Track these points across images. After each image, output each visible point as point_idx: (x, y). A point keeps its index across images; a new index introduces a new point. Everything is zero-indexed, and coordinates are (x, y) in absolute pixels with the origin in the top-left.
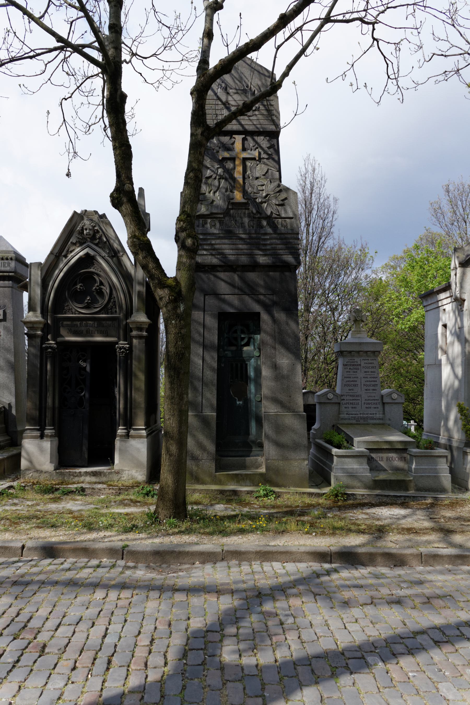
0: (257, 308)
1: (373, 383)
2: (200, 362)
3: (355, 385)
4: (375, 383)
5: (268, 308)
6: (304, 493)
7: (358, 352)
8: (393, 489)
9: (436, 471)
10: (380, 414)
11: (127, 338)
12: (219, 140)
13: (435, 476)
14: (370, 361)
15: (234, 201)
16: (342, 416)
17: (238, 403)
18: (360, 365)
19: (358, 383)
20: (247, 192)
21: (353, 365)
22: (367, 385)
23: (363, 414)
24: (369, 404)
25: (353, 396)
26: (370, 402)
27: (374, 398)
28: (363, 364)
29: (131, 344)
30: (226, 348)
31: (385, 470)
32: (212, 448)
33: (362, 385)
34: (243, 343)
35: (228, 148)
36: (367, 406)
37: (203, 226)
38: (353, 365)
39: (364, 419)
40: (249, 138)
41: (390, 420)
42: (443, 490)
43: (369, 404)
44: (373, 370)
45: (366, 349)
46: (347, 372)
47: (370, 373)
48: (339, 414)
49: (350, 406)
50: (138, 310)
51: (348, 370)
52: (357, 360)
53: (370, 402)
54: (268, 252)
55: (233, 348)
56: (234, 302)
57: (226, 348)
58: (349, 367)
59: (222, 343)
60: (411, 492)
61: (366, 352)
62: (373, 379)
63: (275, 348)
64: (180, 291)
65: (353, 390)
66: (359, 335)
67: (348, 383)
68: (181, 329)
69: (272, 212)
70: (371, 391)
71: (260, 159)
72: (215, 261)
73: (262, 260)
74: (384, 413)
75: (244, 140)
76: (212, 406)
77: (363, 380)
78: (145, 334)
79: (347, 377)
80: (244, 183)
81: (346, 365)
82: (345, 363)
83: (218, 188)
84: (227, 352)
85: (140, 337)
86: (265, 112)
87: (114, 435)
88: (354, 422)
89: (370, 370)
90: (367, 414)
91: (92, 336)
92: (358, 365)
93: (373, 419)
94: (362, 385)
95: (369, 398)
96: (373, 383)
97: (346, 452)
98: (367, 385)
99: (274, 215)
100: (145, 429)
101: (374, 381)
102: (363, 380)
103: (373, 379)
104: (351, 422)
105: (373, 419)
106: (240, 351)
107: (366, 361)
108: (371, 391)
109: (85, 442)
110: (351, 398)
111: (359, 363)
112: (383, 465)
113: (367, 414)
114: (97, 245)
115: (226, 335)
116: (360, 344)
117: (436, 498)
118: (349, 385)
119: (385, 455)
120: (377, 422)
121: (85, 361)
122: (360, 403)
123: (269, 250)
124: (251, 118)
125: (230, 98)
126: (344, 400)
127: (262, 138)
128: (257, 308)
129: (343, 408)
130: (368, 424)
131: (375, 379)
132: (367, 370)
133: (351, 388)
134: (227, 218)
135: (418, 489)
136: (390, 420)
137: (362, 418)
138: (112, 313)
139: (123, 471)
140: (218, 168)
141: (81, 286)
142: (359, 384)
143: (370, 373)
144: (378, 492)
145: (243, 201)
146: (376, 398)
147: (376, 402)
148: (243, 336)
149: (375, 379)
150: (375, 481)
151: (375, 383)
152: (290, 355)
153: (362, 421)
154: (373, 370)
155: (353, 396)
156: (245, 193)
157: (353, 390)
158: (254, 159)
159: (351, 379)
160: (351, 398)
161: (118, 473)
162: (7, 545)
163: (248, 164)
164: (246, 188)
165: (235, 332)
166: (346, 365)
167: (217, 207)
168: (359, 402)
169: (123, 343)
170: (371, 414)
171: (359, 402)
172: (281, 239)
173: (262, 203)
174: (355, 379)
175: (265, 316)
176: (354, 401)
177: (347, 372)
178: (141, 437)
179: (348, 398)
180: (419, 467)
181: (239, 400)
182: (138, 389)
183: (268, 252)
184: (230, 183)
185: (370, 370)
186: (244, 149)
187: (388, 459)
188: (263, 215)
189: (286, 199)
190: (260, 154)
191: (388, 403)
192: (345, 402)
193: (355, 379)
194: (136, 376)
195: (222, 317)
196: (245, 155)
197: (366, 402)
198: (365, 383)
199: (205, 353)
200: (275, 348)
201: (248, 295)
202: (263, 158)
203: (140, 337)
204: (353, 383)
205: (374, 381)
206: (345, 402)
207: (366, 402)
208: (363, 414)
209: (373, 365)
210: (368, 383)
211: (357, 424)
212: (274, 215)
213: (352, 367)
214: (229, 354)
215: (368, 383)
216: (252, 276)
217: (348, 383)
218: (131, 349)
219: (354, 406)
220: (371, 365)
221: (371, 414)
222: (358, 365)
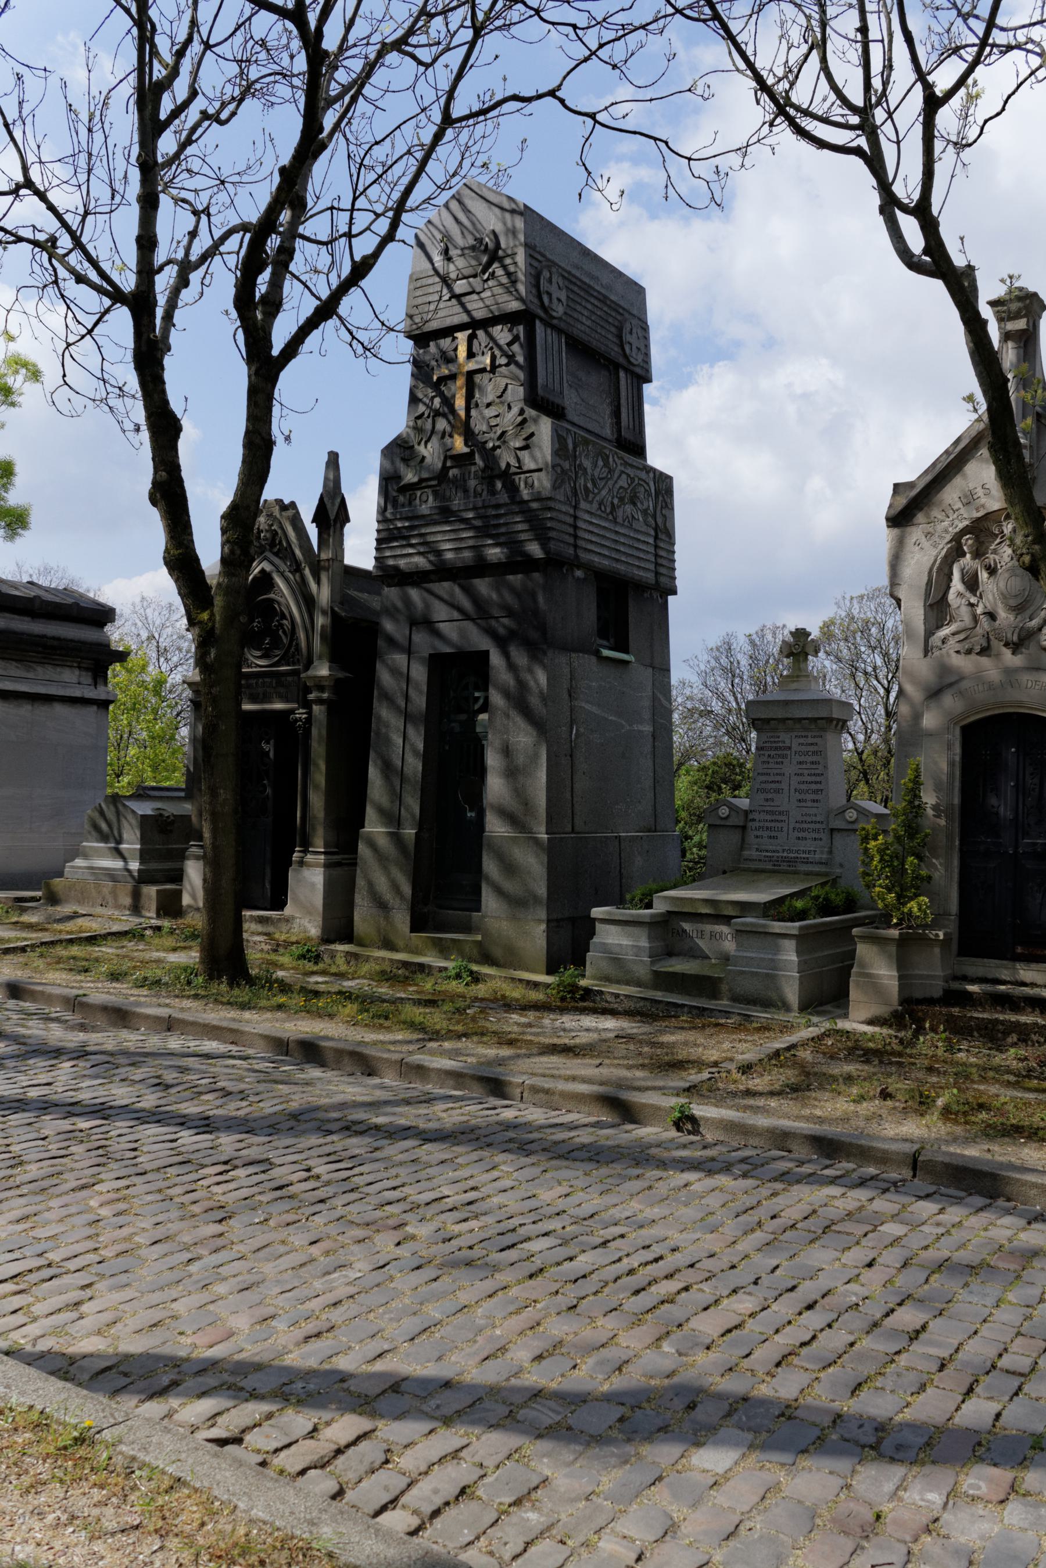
0: (484, 643)
1: (814, 787)
2: (400, 741)
3: (777, 791)
4: (818, 786)
5: (502, 643)
6: (521, 980)
7: (784, 720)
8: (688, 993)
9: (774, 965)
10: (822, 853)
11: (307, 705)
12: (438, 346)
13: (767, 975)
14: (810, 740)
15: (454, 452)
16: (746, 853)
18: (790, 748)
19: (784, 786)
20: (473, 433)
21: (776, 748)
22: (801, 791)
23: (790, 851)
24: (803, 830)
25: (772, 813)
26: (805, 826)
27: (814, 819)
28: (795, 747)
29: (310, 713)
31: (707, 957)
32: (407, 889)
34: (476, 707)
35: (449, 358)
36: (800, 835)
37: (410, 504)
38: (776, 748)
39: (790, 861)
40: (481, 333)
41: (841, 865)
42: (786, 1007)
43: (803, 830)
44: (814, 759)
45: (798, 713)
47: (809, 766)
48: (742, 848)
49: (766, 834)
50: (320, 658)
51: (765, 759)
52: (785, 737)
53: (805, 826)
54: (502, 539)
55: (463, 717)
56: (456, 632)
60: (724, 1003)
61: (800, 720)
62: (813, 779)
63: (508, 716)
64: (213, 628)
65: (772, 800)
66: (794, 686)
67: (763, 786)
68: (211, 687)
69: (508, 465)
70: (809, 804)
71: (494, 367)
72: (420, 562)
73: (494, 553)
74: (830, 852)
75: (471, 339)
77: (795, 780)
78: (325, 695)
80: (468, 415)
83: (433, 431)
85: (320, 701)
86: (504, 280)
87: (290, 863)
88: (770, 867)
89: (810, 759)
90: (797, 852)
91: (271, 702)
93: (807, 862)
95: (805, 818)
96: (814, 787)
97: (609, 913)
98: (801, 791)
99: (513, 470)
100: (324, 853)
101: (816, 783)
102: (795, 780)
103: (813, 779)
104: (761, 866)
105: (807, 862)
106: (472, 722)
107: (802, 740)
108: (809, 804)
109: (268, 871)
110: (769, 817)
112: (703, 947)
113: (797, 852)
114: (276, 554)
116: (787, 703)
117: (749, 1016)
118: (764, 791)
119: (708, 928)
120: (817, 868)
121: (268, 742)
122: (785, 829)
123: (503, 534)
124: (483, 295)
125: (452, 267)
126: (754, 820)
127: (499, 327)
128: (484, 643)
129: (751, 837)
130: (796, 873)
131: (818, 779)
132: (802, 759)
133: (770, 796)
134: (444, 486)
135: (736, 999)
136: (841, 865)
137: (784, 860)
138: (294, 664)
139: (294, 918)
140: (433, 398)
142: (786, 788)
143: (809, 766)
144: (659, 995)
145: (466, 450)
146: (818, 819)
147: (818, 826)
148: (477, 694)
149: (818, 779)
150: (656, 974)
151: (818, 786)
152: (529, 728)
153: (784, 867)
154: (814, 759)
155: (772, 813)
156: (469, 435)
157: (772, 800)
158: (483, 370)
160: (769, 817)
161: (287, 920)
162: (359, 1049)
163: (477, 378)
164: (472, 424)
167: (428, 469)
168: (784, 825)
169: (301, 714)
170: (804, 852)
172: (522, 512)
173: (494, 448)
174: (778, 778)
175: (496, 659)
176: (773, 824)
178: (317, 865)
179: (763, 816)
180: (740, 954)
182: (317, 787)
183: (502, 539)
184: (449, 422)
185: (810, 759)
186: (471, 355)
187: (713, 935)
188: (496, 472)
189: (532, 435)
190: (493, 358)
191: (839, 830)
192: (757, 824)
193: (778, 778)
194: (317, 765)
195: (437, 663)
196: (472, 366)
197: (798, 825)
199: (408, 726)
200: (508, 716)
201: (473, 620)
202: (500, 366)
203: (320, 701)
204: (773, 786)
205: (816, 783)
206: (757, 824)
207: (798, 825)
208: (790, 851)
209: (815, 748)
210: (804, 787)
211: (774, 872)
212: (513, 470)
213: (773, 753)
215: (804, 787)
216: (483, 586)
217: (763, 786)
218: (309, 720)
219: (773, 834)
220: (811, 748)
221: (804, 852)
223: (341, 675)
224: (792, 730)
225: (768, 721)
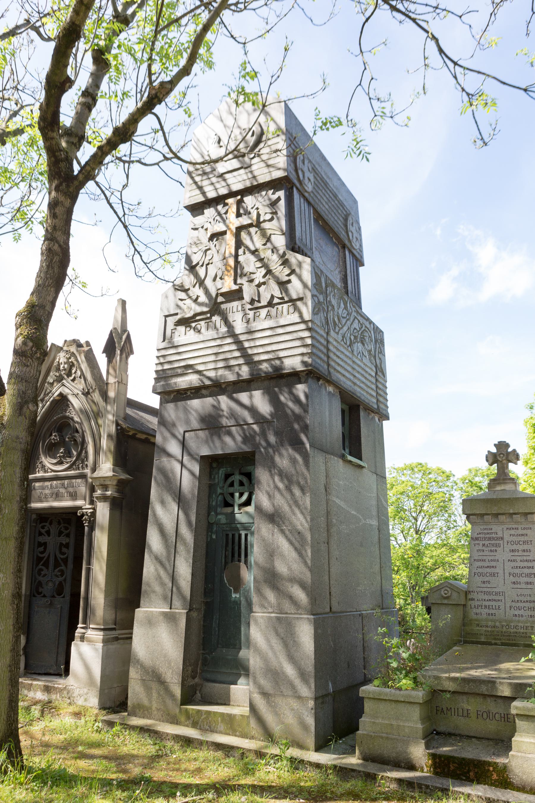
1: (526, 571)
3: (493, 575)
14: (520, 532)
17: (234, 596)
18: (502, 538)
21: (490, 539)
25: (489, 593)
27: (529, 599)
28: (507, 537)
33: (507, 575)
38: (490, 539)
44: (526, 547)
46: (479, 550)
47: (520, 553)
51: (481, 547)
57: (219, 510)
58: (481, 543)
59: (214, 503)
62: (526, 564)
65: (489, 582)
67: (480, 570)
70: (524, 586)
76: (183, 598)
77: (508, 565)
78: (109, 493)
79: (478, 560)
81: (477, 539)
82: (476, 535)
84: (219, 517)
89: (521, 547)
92: (498, 539)
94: (507, 575)
95: (520, 598)
96: (526, 571)
101: (529, 568)
103: (526, 564)
107: (512, 532)
108: (524, 586)
110: (486, 597)
111: (500, 535)
115: (219, 491)
118: (481, 574)
126: (473, 599)
132: (515, 547)
141: (55, 436)
142: (501, 572)
143: (520, 553)
154: (526, 547)
155: (489, 593)
157: (489, 582)
165: (232, 485)
166: (477, 539)
168: (501, 604)
171: (501, 604)
174: (493, 564)
176: (491, 603)
177: (479, 550)
181: (235, 592)
185: (521, 547)
193: (493, 564)
198: (512, 571)
203: (104, 498)
204: (488, 570)
205: (529, 568)
207: (514, 604)
209: (526, 538)
210: (517, 571)
213: (487, 543)
214: (222, 519)
215: (517, 571)
217: (480, 570)
220: (522, 539)
222: (498, 539)
223: (124, 476)
224: (502, 523)
225: (482, 515)
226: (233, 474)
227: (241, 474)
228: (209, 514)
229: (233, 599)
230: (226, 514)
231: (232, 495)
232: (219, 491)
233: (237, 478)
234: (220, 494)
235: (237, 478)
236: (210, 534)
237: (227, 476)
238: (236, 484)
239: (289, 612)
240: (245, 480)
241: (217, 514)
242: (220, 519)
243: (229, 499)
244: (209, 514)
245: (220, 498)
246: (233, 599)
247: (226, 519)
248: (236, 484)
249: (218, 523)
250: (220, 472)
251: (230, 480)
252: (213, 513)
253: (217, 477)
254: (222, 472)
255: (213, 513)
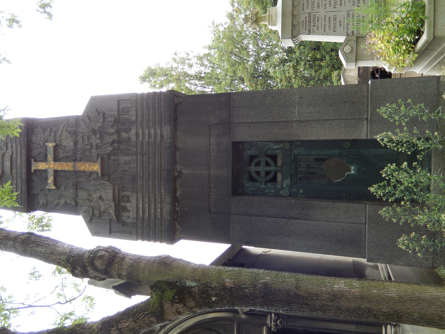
3: (335, 19)
7: (293, 16)
17: (353, 172)
18: (310, 13)
28: (309, 10)
30: (279, 186)
33: (335, 9)
38: (310, 22)
46: (318, 29)
51: (316, 28)
52: (303, 17)
57: (279, 186)
58: (312, 28)
59: (273, 191)
65: (340, 21)
67: (332, 28)
79: (325, 29)
81: (309, 31)
82: (307, 31)
84: (285, 186)
92: (310, 17)
94: (335, 9)
107: (305, 7)
111: (307, 15)
118: (335, 27)
126: (353, 32)
132: (316, 5)
133: (338, 24)
142: (333, 13)
145: (99, 161)
157: (340, 21)
159: (327, 24)
165: (258, 173)
166: (309, 31)
177: (318, 29)
181: (350, 171)
198: (332, 6)
204: (332, 22)
207: (356, 4)
213: (312, 24)
217: (332, 28)
222: (310, 17)
225: (293, 26)
226: (250, 172)
227: (250, 165)
228: (281, 196)
229: (356, 173)
230: (283, 179)
231: (267, 173)
232: (263, 186)
233: (253, 168)
234: (265, 185)
235: (253, 168)
236: (299, 195)
237: (252, 179)
238: (258, 169)
239: (366, 104)
240: (255, 161)
241: (282, 188)
242: (287, 185)
243: (270, 176)
244: (281, 196)
245: (269, 185)
246: (356, 173)
247: (287, 179)
248: (258, 169)
249: (291, 187)
250: (247, 185)
251: (254, 175)
252: (281, 192)
253: (250, 189)
254: (248, 184)
255: (281, 192)
